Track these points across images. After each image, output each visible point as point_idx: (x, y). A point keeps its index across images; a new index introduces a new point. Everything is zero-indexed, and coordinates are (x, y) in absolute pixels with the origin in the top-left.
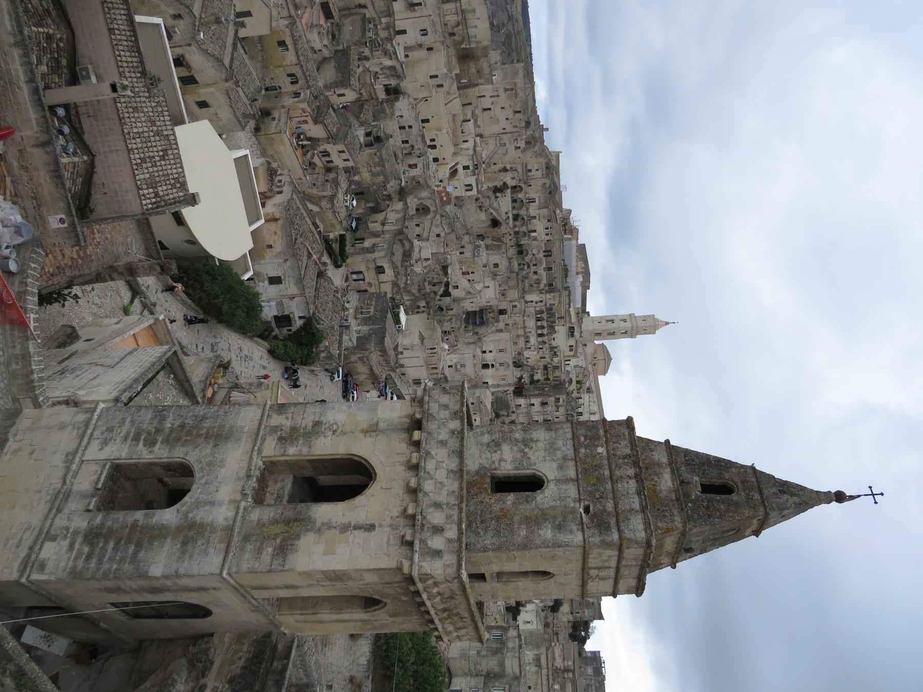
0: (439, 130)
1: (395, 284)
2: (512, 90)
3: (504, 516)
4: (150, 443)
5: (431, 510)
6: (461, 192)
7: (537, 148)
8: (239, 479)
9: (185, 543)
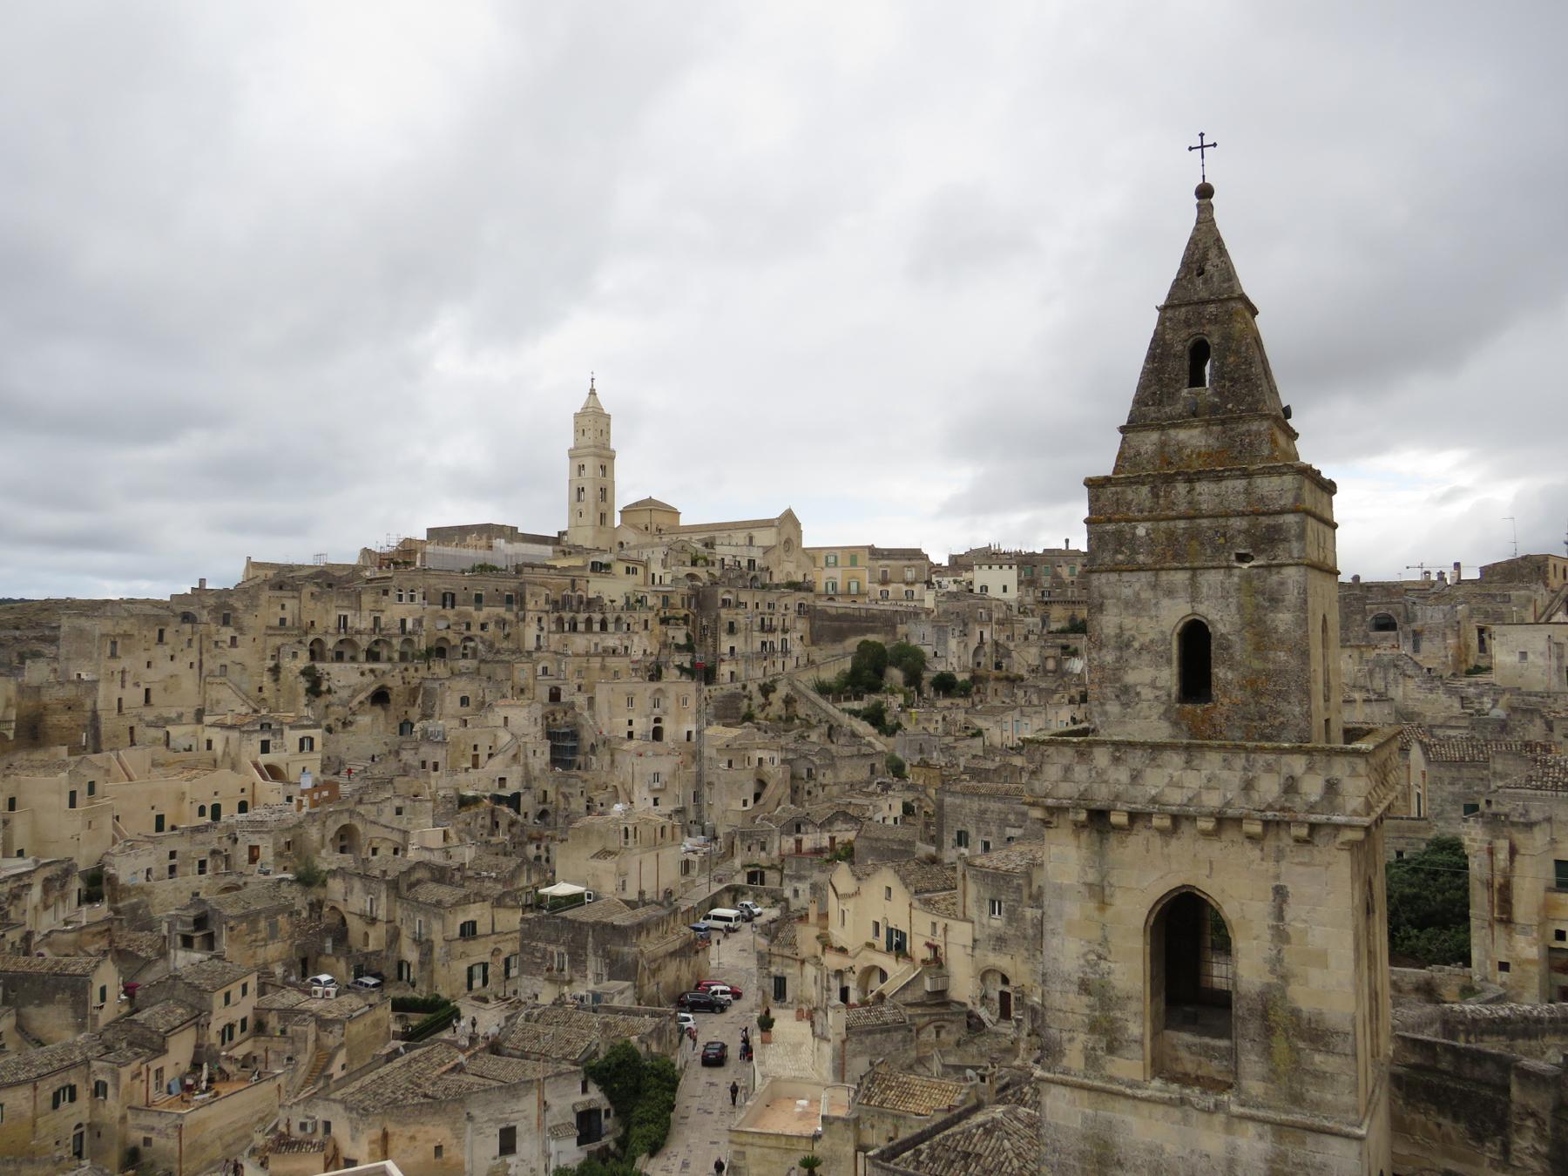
0: (182, 796)
1: (499, 902)
2: (114, 643)
3: (1253, 685)
5: (1255, 796)
6: (314, 761)
7: (238, 605)
8: (1186, 1120)
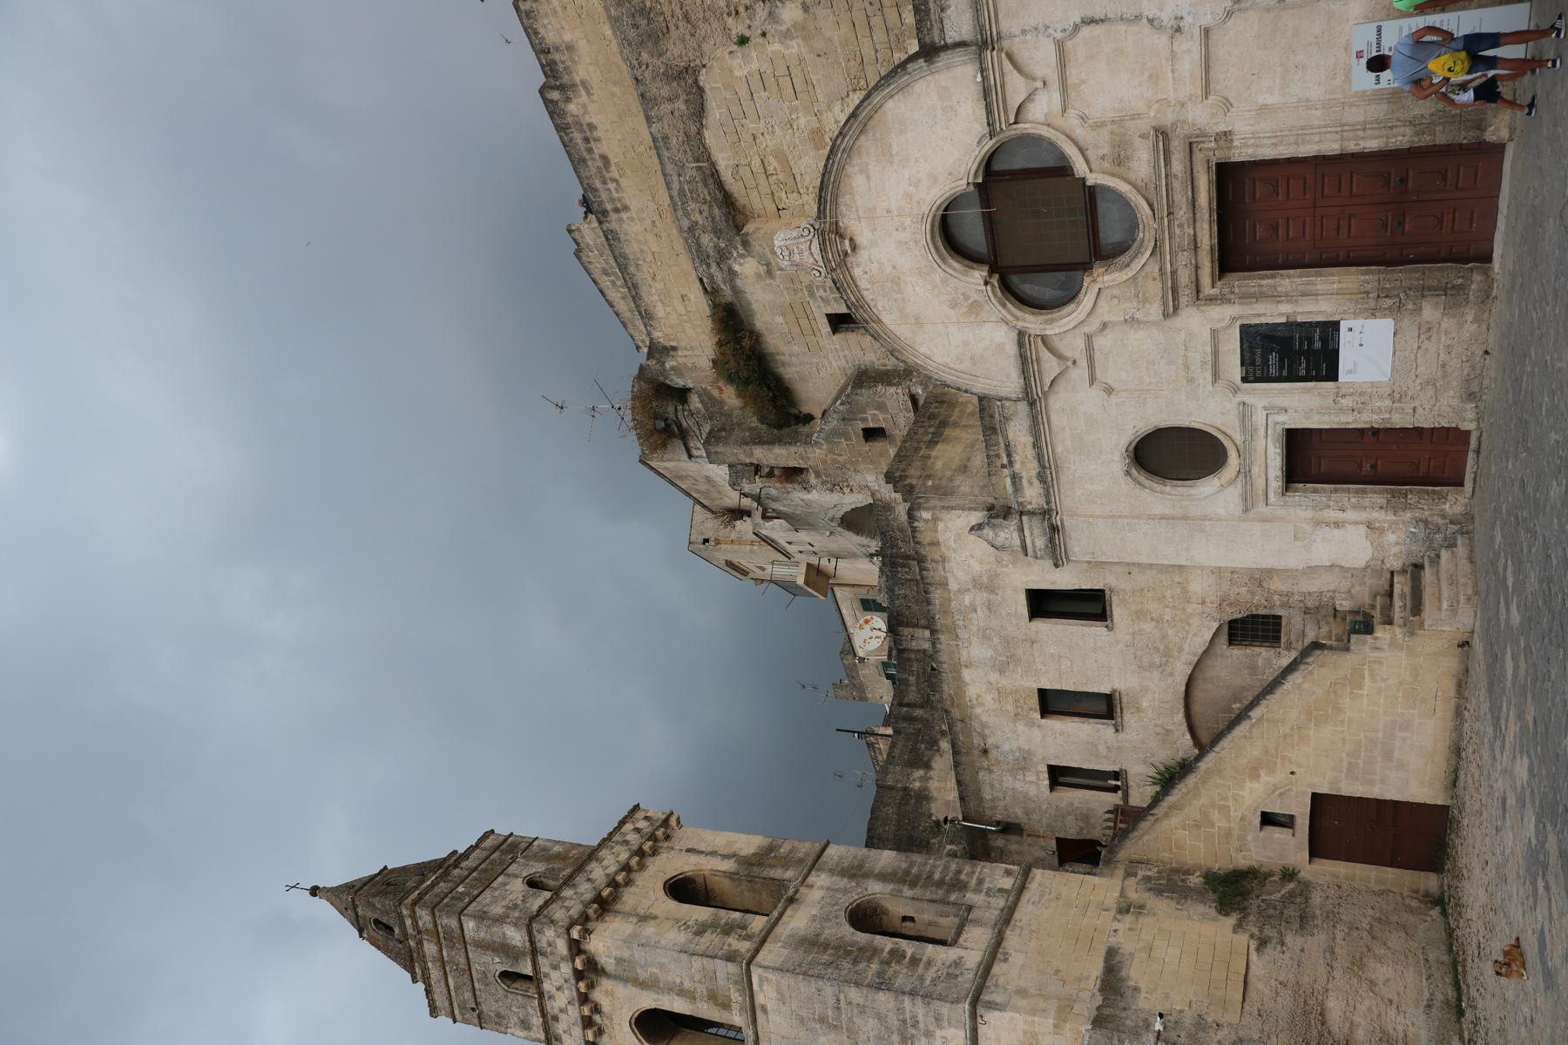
4: (897, 955)
9: (861, 866)
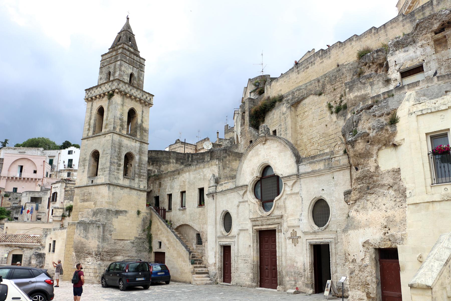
4: (119, 165)
9: (142, 153)
